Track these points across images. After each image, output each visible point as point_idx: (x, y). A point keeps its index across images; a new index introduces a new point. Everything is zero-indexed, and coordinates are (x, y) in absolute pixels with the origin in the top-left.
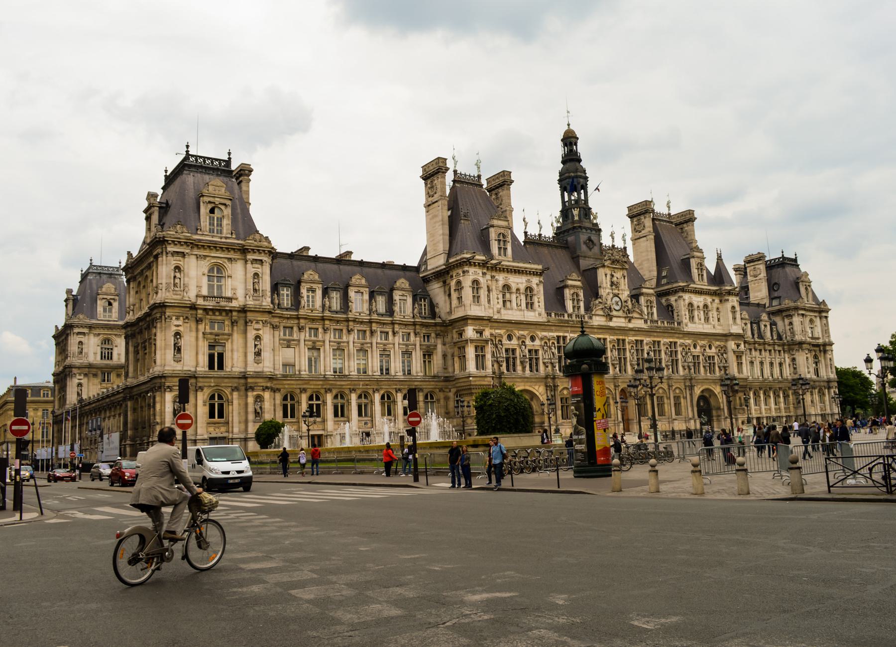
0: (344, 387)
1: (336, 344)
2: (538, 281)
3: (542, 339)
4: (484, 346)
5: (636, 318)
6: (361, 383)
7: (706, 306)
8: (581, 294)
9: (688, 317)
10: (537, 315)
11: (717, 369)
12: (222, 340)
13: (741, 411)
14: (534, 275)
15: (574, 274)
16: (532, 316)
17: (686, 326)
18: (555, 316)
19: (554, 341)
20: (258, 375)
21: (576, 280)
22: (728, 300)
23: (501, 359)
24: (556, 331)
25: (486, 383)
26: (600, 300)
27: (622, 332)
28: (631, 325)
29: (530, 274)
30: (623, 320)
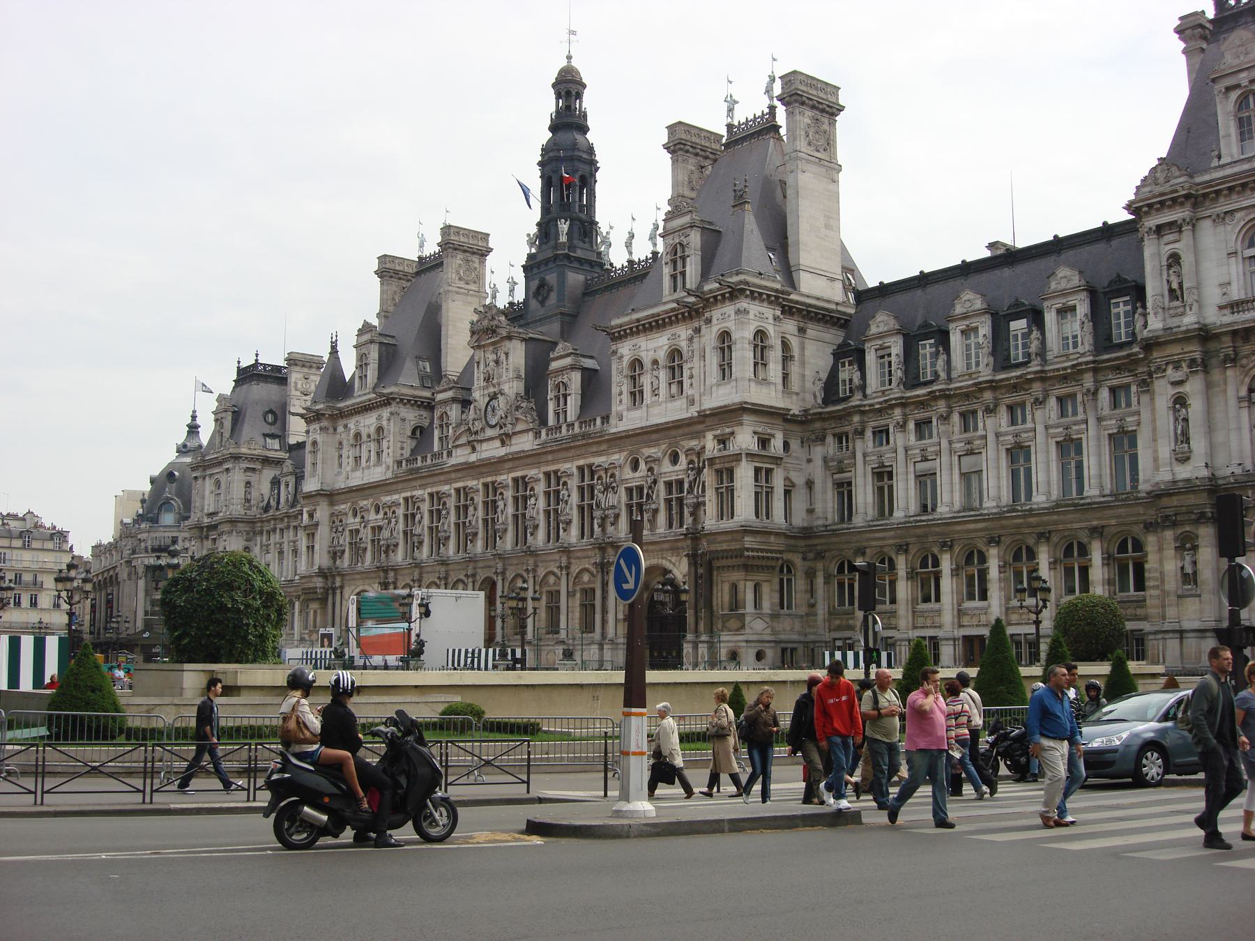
5: (514, 434)
7: (675, 354)
9: (626, 397)
13: (733, 623)
24: (403, 490)
25: (312, 585)
28: (502, 452)
29: (378, 407)
30: (497, 443)
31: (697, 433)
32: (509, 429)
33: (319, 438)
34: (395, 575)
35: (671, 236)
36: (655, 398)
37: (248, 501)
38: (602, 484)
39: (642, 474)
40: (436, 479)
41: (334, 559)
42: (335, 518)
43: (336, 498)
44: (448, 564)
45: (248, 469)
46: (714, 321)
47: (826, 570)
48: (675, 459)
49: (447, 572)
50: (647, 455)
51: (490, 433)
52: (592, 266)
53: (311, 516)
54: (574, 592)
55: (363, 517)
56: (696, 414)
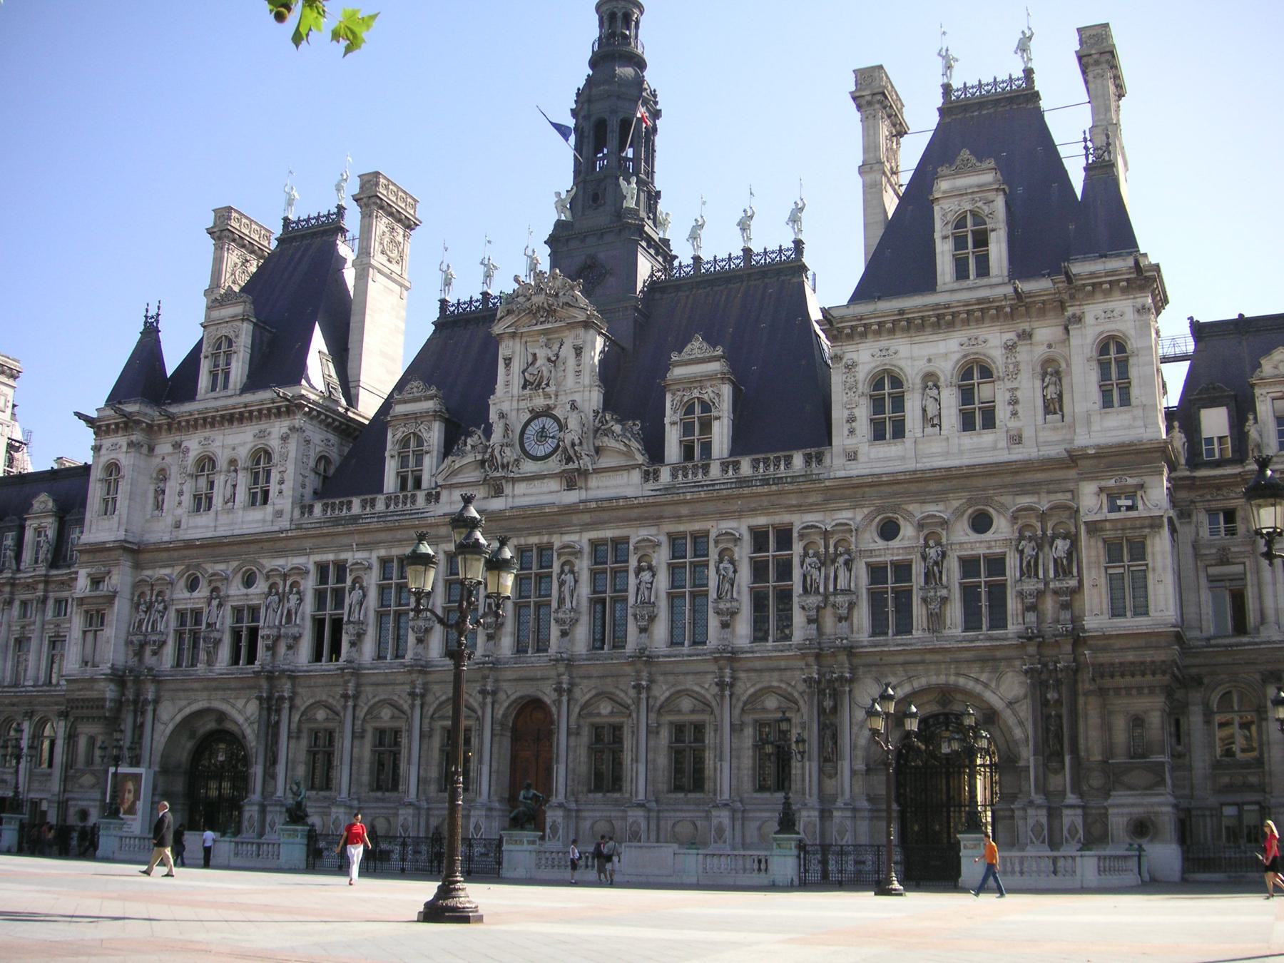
3: (268, 577)
5: (596, 471)
8: (434, 435)
9: (863, 426)
10: (269, 518)
11: (1013, 605)
15: (416, 384)
16: (257, 521)
17: (852, 456)
18: (325, 511)
19: (298, 579)
22: (1078, 319)
23: (154, 638)
24: (313, 550)
25: (95, 694)
28: (572, 497)
30: (554, 485)
31: (1032, 484)
32: (586, 463)
33: (126, 460)
34: (294, 686)
35: (956, 200)
36: (929, 430)
38: (816, 554)
39: (906, 543)
40: (399, 535)
41: (139, 654)
43: (148, 556)
44: (426, 673)
46: (1089, 319)
47: (1206, 705)
48: (981, 523)
49: (426, 687)
50: (919, 516)
51: (529, 467)
52: (657, 253)
53: (96, 582)
54: (742, 725)
56: (1065, 455)
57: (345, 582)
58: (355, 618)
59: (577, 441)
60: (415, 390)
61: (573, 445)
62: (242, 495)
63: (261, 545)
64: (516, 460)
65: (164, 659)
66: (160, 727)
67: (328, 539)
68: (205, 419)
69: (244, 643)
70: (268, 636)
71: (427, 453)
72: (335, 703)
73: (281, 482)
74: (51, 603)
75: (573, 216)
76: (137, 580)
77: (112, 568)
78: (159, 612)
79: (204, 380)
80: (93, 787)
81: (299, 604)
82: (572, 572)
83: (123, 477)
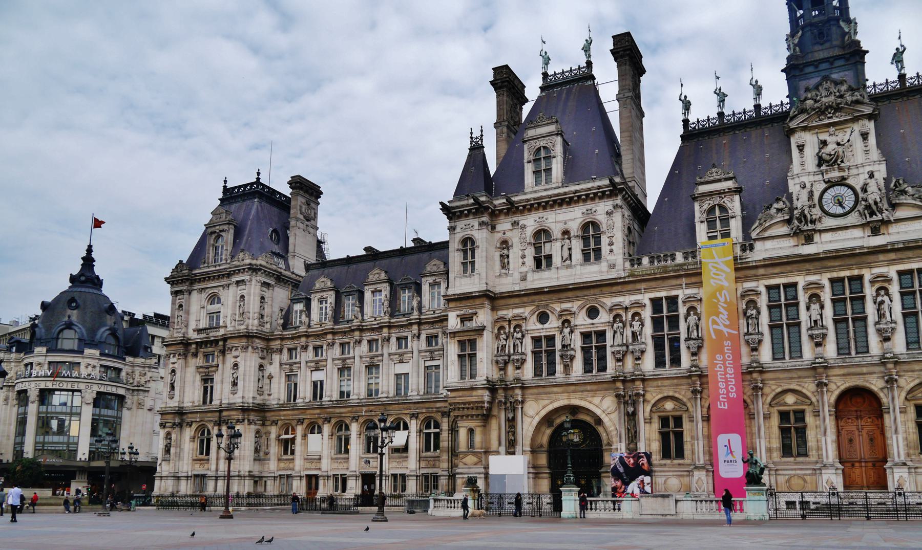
0: (343, 415)
1: (340, 362)
2: (611, 208)
4: (476, 339)
5: (898, 221)
6: (364, 409)
8: (735, 205)
12: (211, 372)
14: (601, 198)
15: (714, 170)
18: (652, 262)
19: (638, 310)
20: (231, 408)
21: (719, 181)
24: (647, 290)
26: (780, 205)
27: (848, 261)
30: (858, 233)
32: (886, 215)
33: (480, 236)
34: (643, 385)
37: (262, 316)
42: (506, 325)
43: (502, 302)
45: (265, 283)
51: (829, 222)
53: (464, 319)
55: (565, 322)
57: (677, 310)
58: (694, 335)
59: (878, 200)
60: (714, 174)
61: (876, 203)
62: (577, 255)
63: (600, 289)
64: (820, 218)
65: (525, 372)
66: (527, 420)
67: (659, 282)
68: (539, 204)
69: (594, 357)
70: (618, 352)
71: (732, 217)
72: (681, 397)
73: (611, 244)
74: (393, 340)
75: (801, 51)
76: (496, 317)
77: (477, 310)
78: (519, 339)
79: (529, 178)
80: (475, 464)
81: (642, 328)
82: (887, 294)
83: (478, 247)
